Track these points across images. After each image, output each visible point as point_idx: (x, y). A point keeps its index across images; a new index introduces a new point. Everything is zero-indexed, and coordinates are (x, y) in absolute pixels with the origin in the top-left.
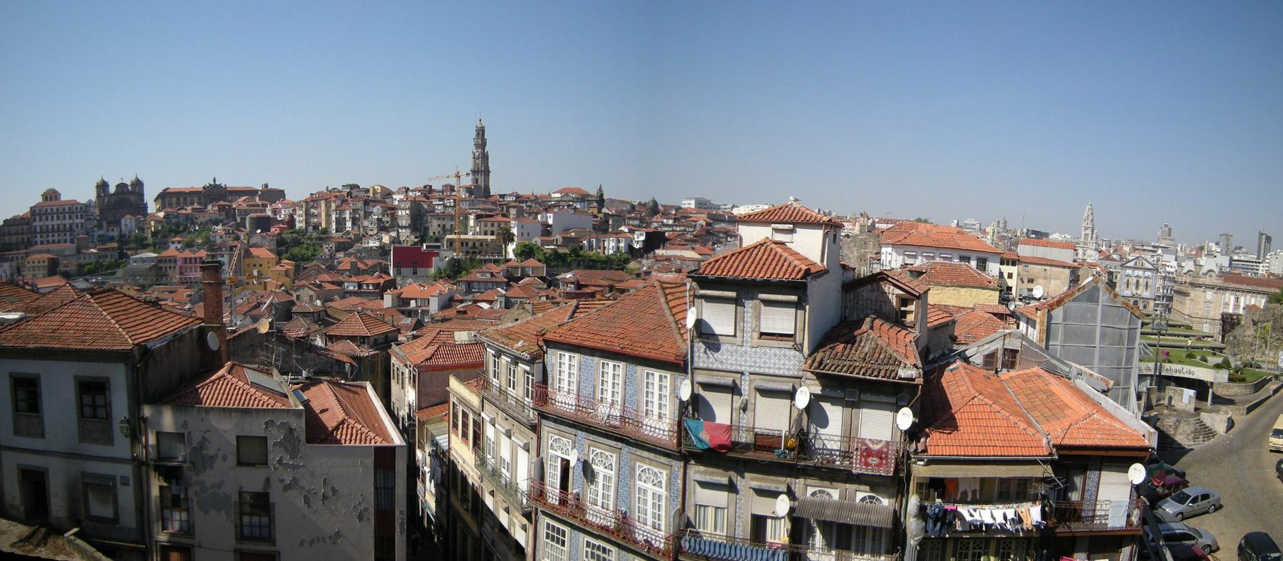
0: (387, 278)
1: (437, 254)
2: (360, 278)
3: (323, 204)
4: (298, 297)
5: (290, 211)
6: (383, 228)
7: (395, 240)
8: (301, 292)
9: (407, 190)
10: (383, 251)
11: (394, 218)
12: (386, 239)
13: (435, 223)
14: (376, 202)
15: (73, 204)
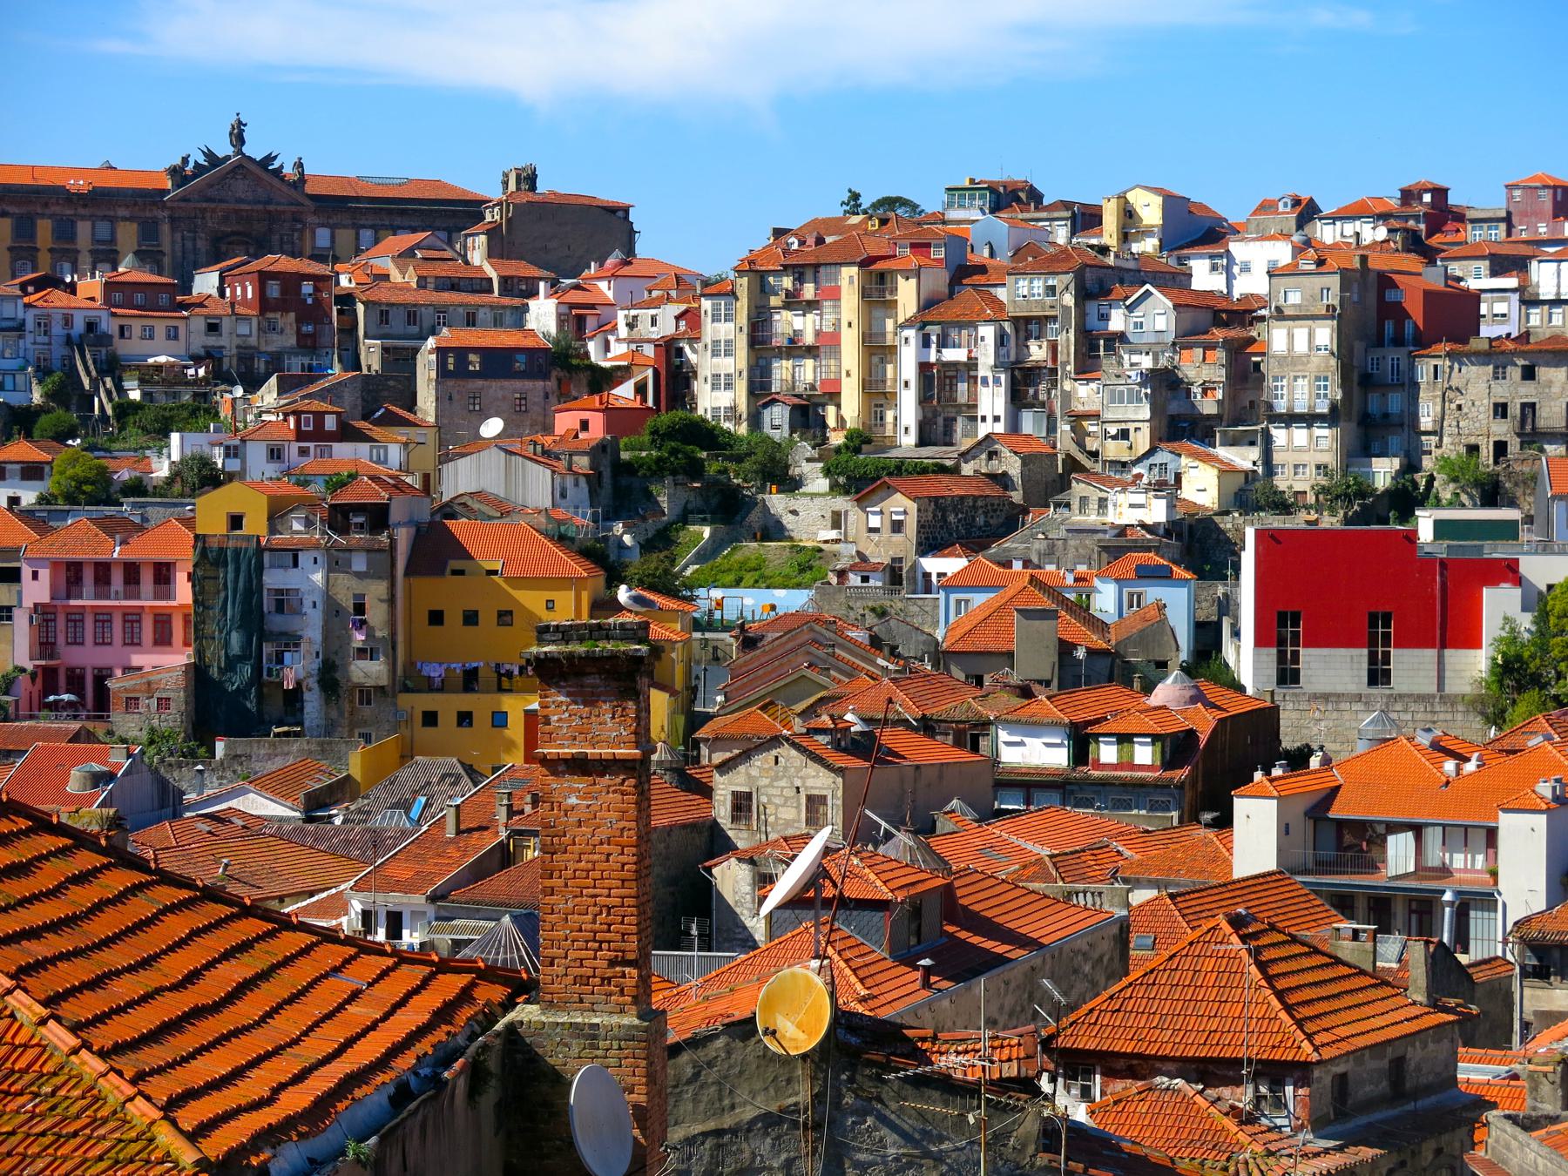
0: (1236, 707)
1: (1508, 572)
2: (1088, 703)
3: (849, 277)
4: (742, 805)
5: (666, 322)
6: (1180, 425)
7: (1250, 493)
8: (754, 774)
9: (1307, 212)
10: (1197, 546)
11: (1245, 371)
12: (1201, 486)
13: (1476, 383)
14: (1138, 275)
15: (192, 280)
